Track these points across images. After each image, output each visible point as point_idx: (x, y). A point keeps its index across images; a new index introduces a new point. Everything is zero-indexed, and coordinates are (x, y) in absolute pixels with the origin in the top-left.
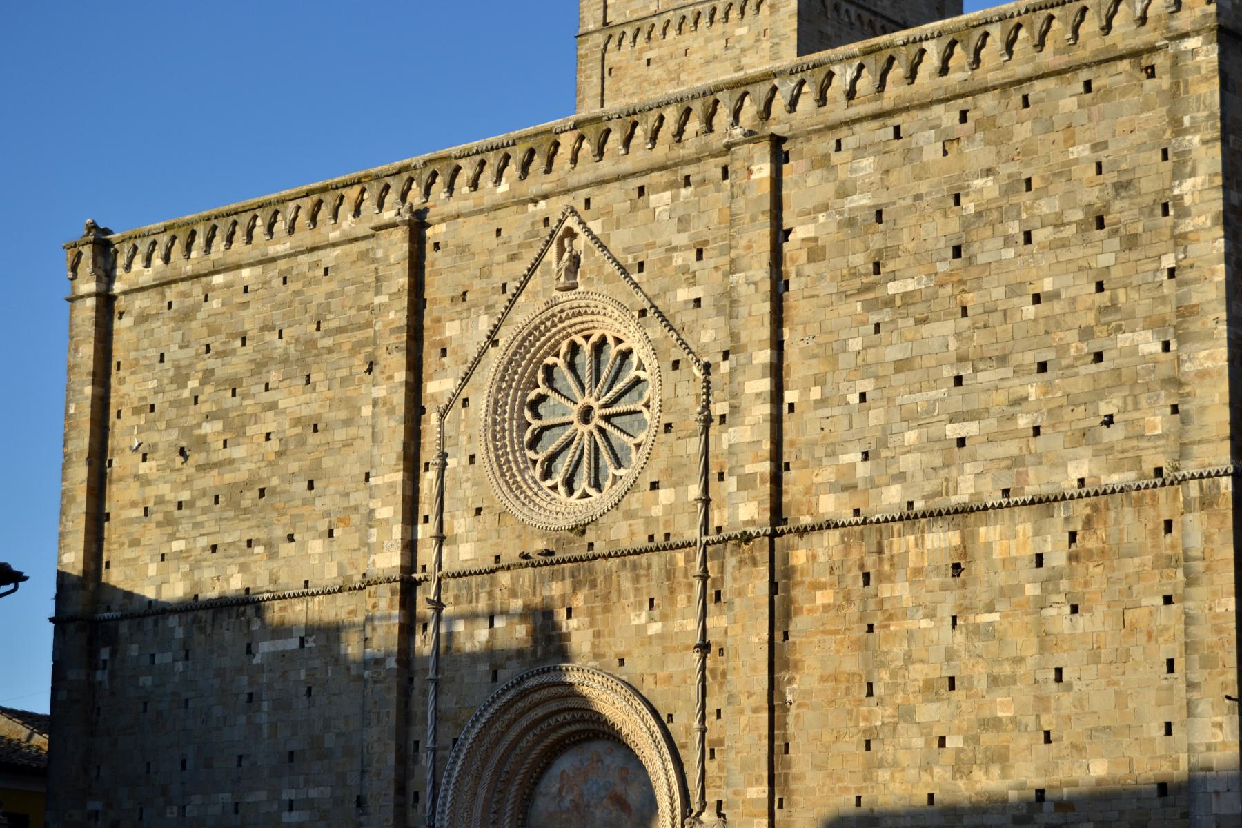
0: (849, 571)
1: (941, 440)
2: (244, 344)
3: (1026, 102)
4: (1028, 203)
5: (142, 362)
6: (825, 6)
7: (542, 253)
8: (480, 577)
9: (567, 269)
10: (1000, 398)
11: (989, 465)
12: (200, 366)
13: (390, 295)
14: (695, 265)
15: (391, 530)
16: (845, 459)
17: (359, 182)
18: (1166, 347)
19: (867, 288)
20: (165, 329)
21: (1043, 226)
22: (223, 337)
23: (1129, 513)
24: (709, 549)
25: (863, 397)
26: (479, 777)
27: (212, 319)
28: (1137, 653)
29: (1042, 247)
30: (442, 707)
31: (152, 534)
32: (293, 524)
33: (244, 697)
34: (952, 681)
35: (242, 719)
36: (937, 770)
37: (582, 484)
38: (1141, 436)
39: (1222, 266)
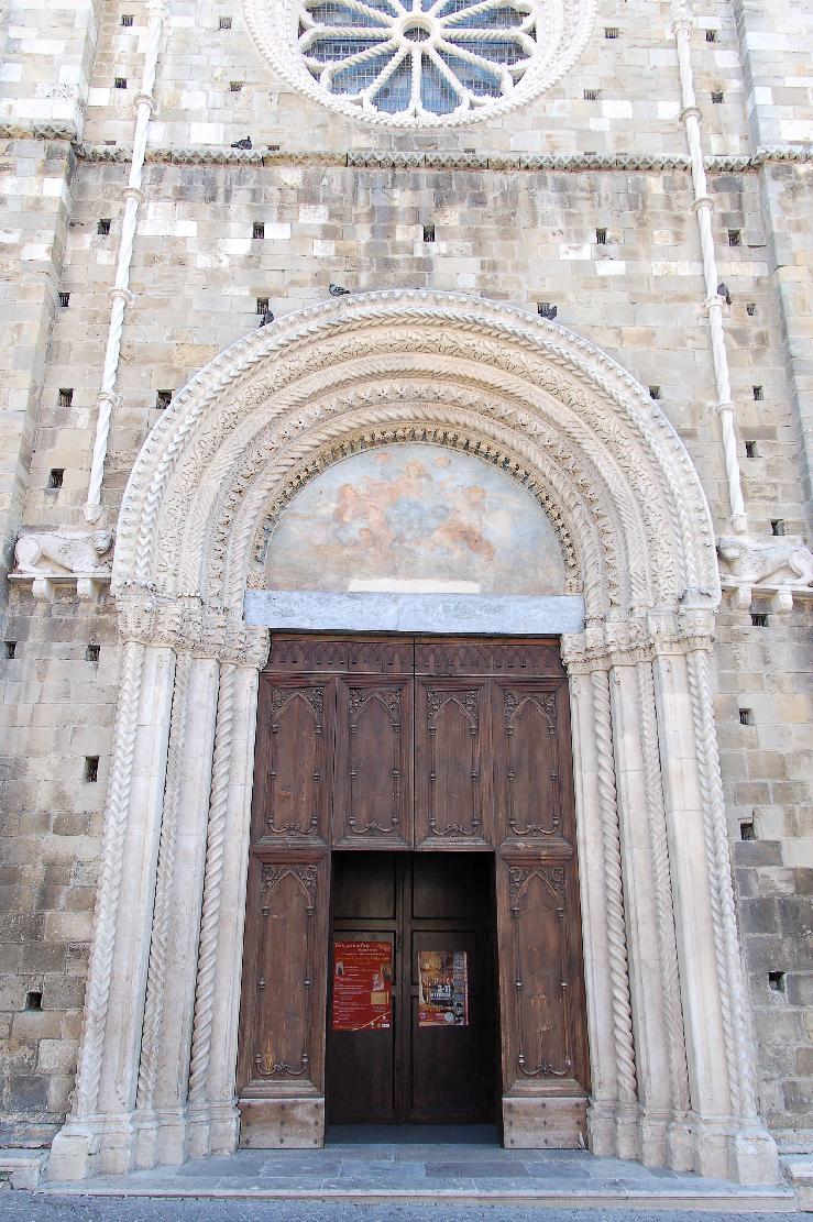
8: (234, 170)
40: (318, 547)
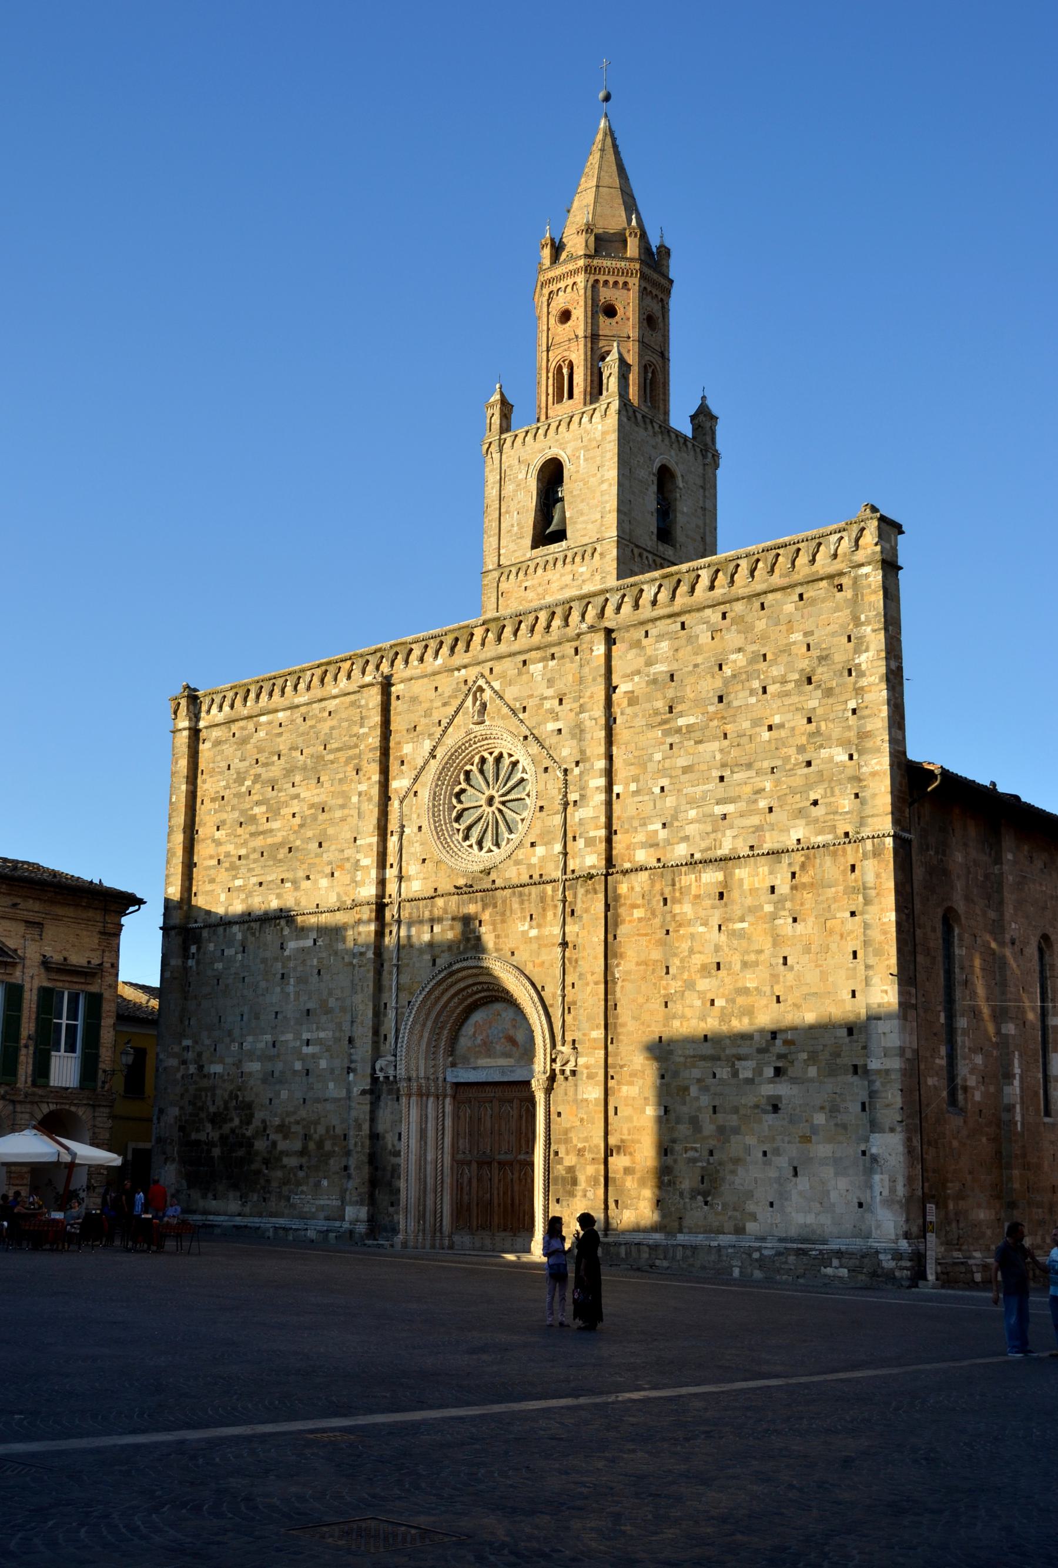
0: (654, 897)
1: (712, 815)
2: (279, 759)
3: (763, 607)
4: (764, 669)
5: (217, 770)
6: (633, 554)
7: (462, 703)
8: (425, 901)
9: (479, 711)
10: (748, 789)
11: (741, 831)
12: (252, 772)
13: (369, 728)
14: (558, 708)
15: (370, 873)
16: (651, 828)
17: (350, 659)
18: (851, 757)
19: (665, 722)
20: (231, 750)
21: (774, 683)
22: (266, 754)
23: (828, 861)
24: (567, 883)
25: (662, 789)
26: (424, 1025)
27: (260, 743)
28: (833, 947)
29: (773, 696)
30: (401, 981)
31: (223, 876)
32: (309, 869)
33: (279, 976)
34: (718, 964)
35: (278, 989)
36: (709, 1020)
37: (488, 843)
38: (836, 813)
39: (886, 707)
40: (469, 1048)
